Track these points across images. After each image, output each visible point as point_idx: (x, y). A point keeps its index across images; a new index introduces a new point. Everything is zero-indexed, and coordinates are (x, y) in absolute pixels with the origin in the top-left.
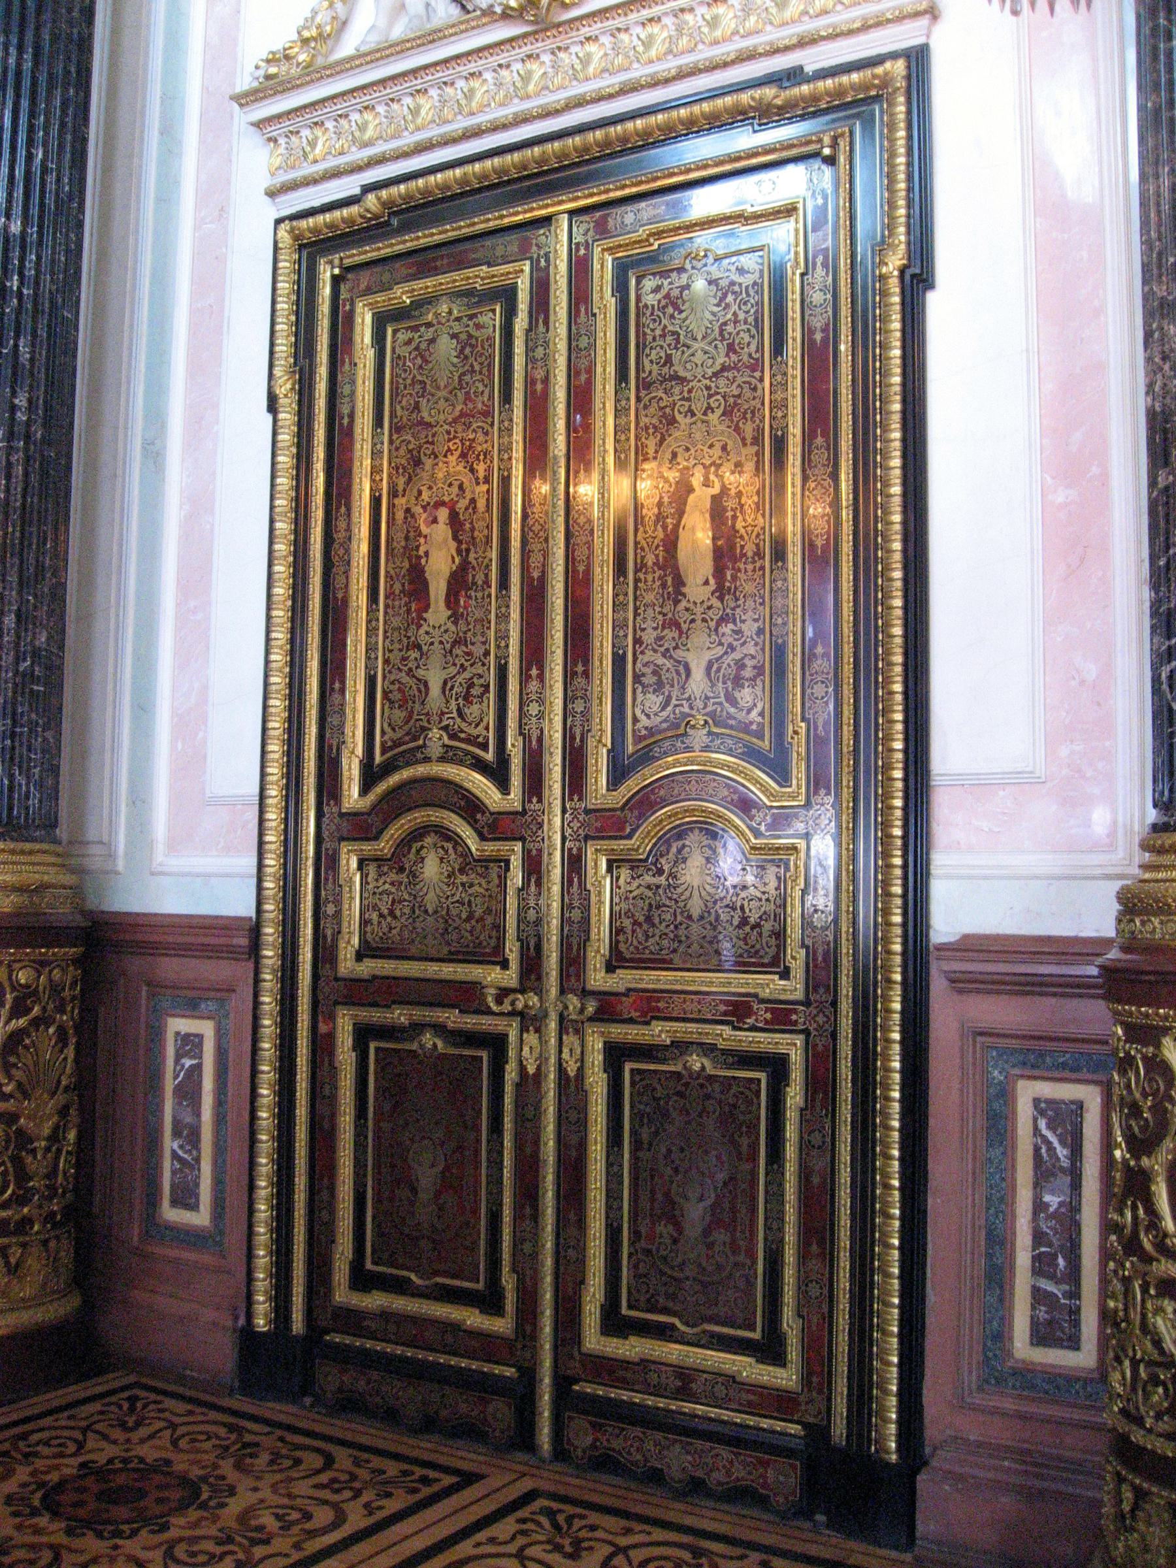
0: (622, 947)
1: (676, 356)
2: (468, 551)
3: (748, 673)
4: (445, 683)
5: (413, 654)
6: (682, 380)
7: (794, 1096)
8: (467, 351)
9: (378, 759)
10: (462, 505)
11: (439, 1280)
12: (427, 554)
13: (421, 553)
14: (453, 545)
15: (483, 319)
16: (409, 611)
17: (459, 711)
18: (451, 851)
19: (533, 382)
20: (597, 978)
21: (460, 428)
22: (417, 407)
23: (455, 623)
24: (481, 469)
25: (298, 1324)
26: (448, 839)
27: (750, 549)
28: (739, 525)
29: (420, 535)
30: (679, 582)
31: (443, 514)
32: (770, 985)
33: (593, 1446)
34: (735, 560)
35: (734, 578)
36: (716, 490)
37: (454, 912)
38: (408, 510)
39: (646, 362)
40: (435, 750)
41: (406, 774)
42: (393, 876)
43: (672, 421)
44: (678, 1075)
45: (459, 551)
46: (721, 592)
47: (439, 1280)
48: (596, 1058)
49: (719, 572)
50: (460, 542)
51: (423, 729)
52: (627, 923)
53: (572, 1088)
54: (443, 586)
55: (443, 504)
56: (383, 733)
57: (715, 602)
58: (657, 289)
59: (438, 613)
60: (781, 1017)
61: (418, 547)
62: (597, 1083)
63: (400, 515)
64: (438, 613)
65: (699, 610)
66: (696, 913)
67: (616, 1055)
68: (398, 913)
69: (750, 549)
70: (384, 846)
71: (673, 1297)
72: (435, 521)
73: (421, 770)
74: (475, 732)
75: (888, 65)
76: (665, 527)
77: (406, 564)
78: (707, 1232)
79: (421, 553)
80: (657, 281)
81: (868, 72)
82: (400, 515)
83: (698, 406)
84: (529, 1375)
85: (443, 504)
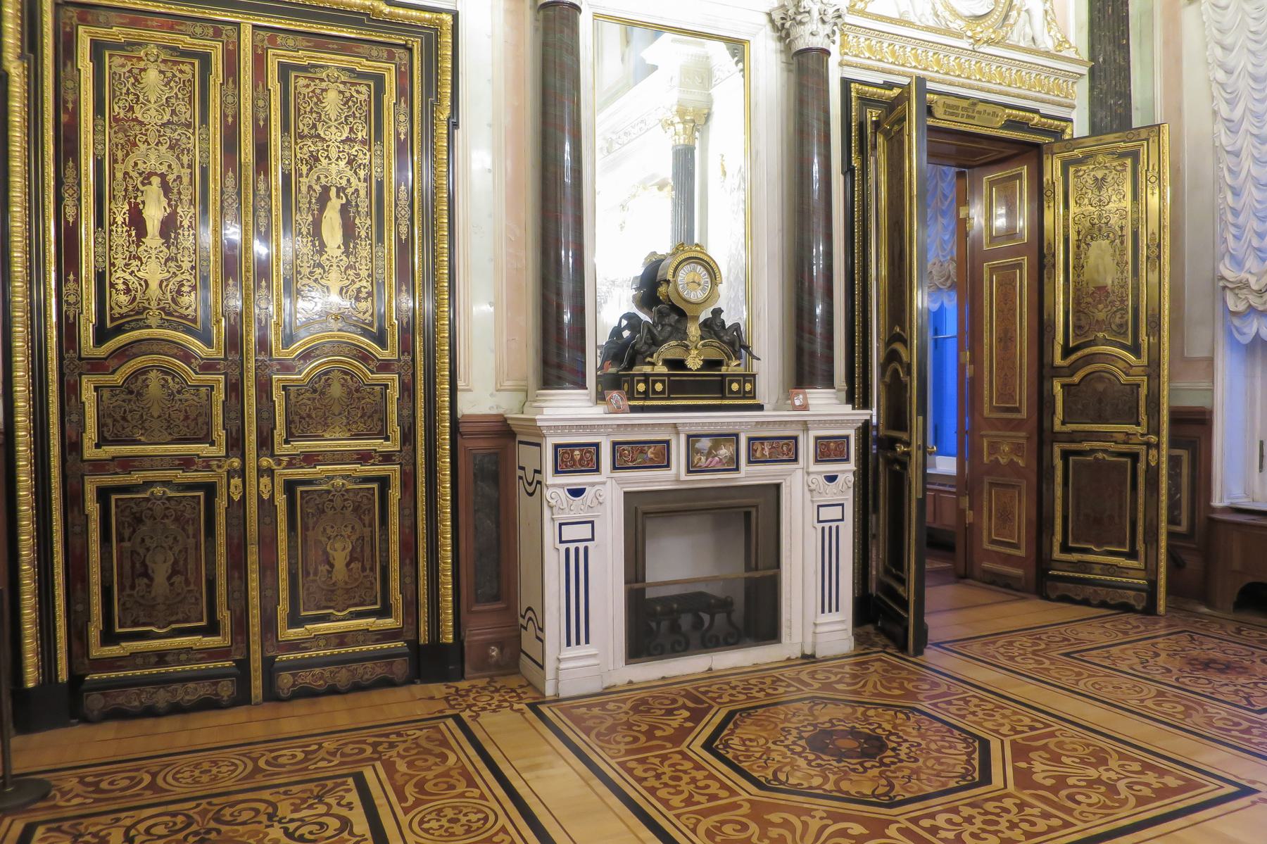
0: (106, 434)
1: (319, 126)
2: (176, 206)
3: (363, 295)
4: (161, 282)
5: (135, 263)
6: (323, 140)
7: (395, 494)
8: (172, 84)
9: (109, 325)
10: (171, 178)
11: (174, 626)
12: (143, 202)
13: (139, 200)
14: (164, 202)
15: (187, 68)
16: (130, 236)
17: (173, 299)
18: (170, 380)
19: (226, 116)
20: (282, 449)
21: (168, 131)
22: (131, 109)
23: (168, 248)
24: (185, 159)
25: (63, 676)
26: (168, 374)
27: (363, 234)
28: (357, 221)
29: (138, 190)
30: (323, 245)
31: (156, 181)
32: (378, 444)
33: (294, 685)
34: (355, 238)
35: (355, 248)
36: (344, 201)
37: (173, 416)
38: (126, 173)
39: (301, 126)
40: (153, 321)
41: (135, 335)
42: (123, 396)
43: (317, 159)
44: (328, 492)
45: (169, 205)
46: (347, 253)
47: (174, 626)
48: (279, 487)
49: (346, 244)
50: (170, 200)
51: (145, 309)
52: (109, 421)
53: (266, 506)
54: (157, 225)
55: (156, 174)
56: (111, 309)
57: (344, 257)
58: (307, 86)
59: (153, 239)
60: (387, 458)
61: (136, 198)
62: (281, 500)
63: (119, 175)
64: (153, 239)
65: (334, 260)
66: (156, 415)
67: (290, 486)
68: (129, 418)
69: (363, 234)
70: (118, 378)
71: (331, 600)
72: (150, 183)
73: (144, 333)
74: (186, 313)
75: (444, 16)
76: (313, 215)
77: (127, 207)
78: (348, 565)
79: (139, 200)
80: (306, 82)
81: (435, 15)
82: (119, 175)
83: (334, 155)
84: (244, 665)
85: (156, 174)
